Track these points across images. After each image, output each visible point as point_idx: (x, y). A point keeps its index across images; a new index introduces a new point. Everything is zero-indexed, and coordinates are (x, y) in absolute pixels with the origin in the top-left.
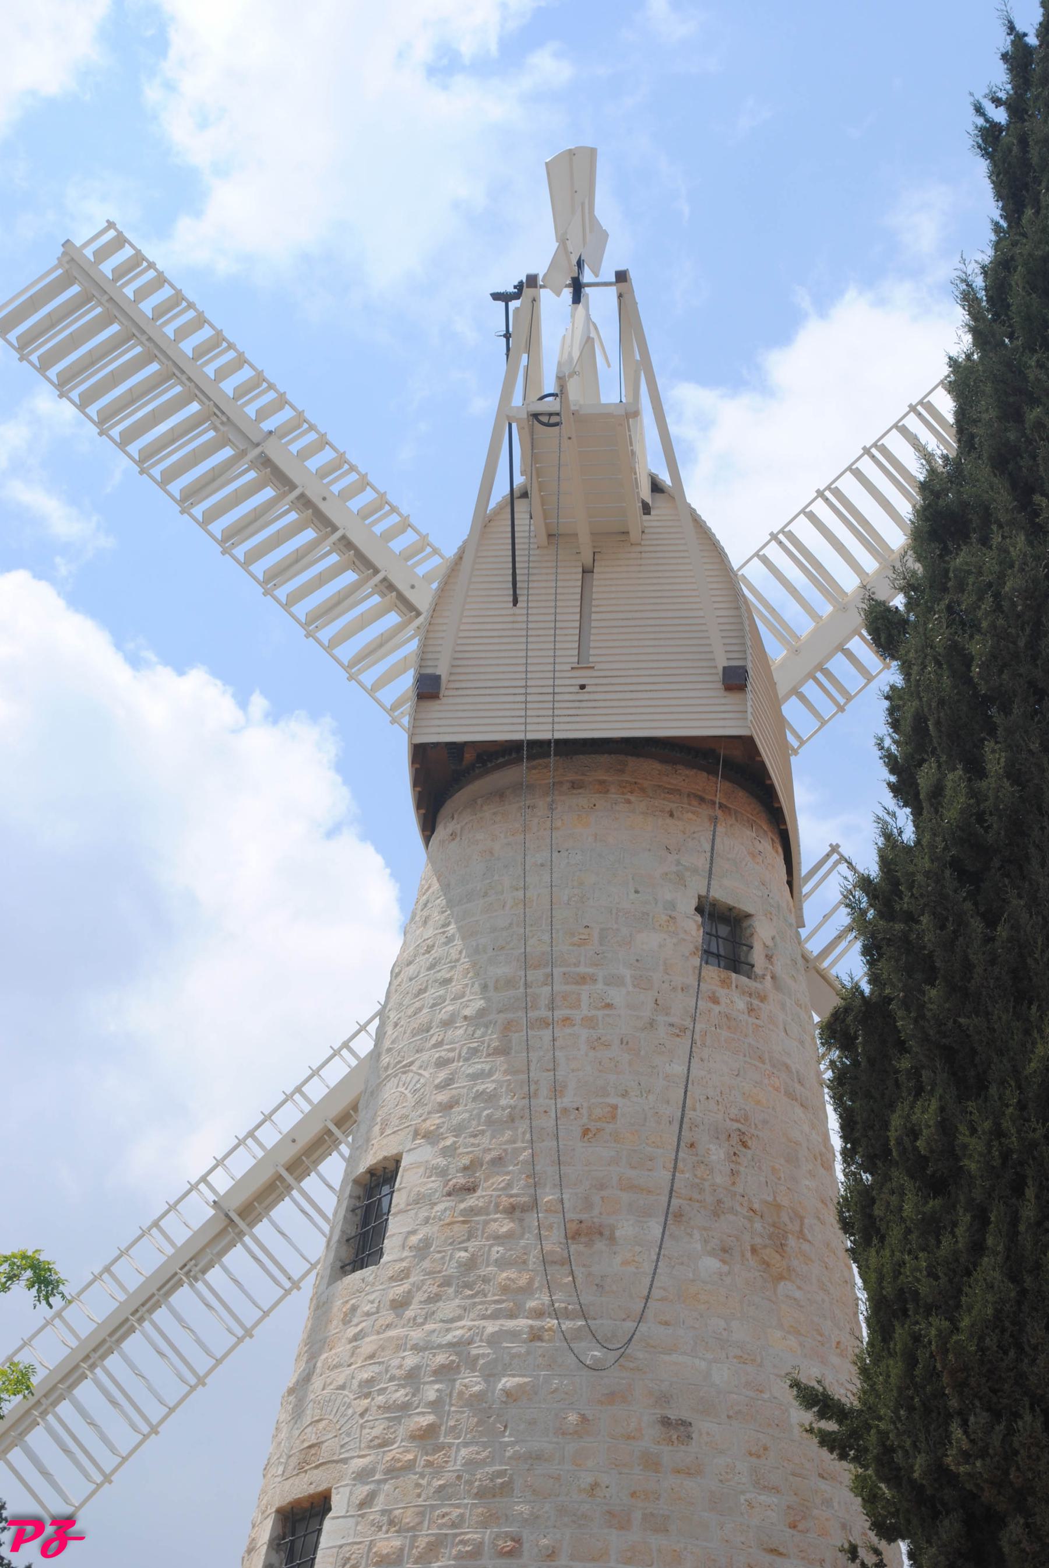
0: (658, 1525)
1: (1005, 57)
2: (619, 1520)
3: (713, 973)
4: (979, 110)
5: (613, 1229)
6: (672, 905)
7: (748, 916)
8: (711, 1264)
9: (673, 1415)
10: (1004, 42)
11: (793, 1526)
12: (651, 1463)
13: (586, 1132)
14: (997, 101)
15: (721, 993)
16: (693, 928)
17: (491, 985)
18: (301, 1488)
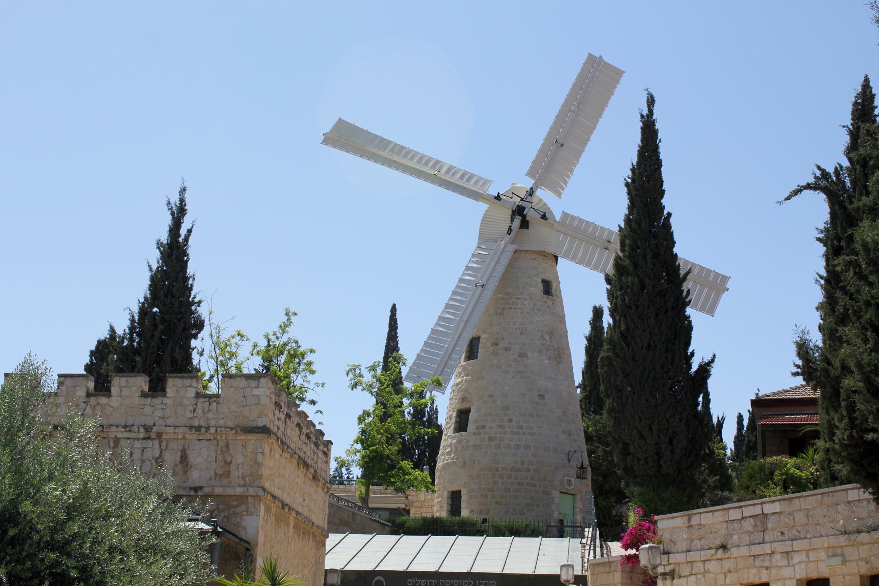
0: (538, 416)
1: (631, 169)
2: (532, 415)
3: (545, 296)
4: (625, 180)
5: (527, 354)
6: (536, 281)
7: (551, 281)
8: (547, 362)
9: (541, 394)
10: (631, 167)
11: (564, 415)
12: (537, 404)
13: (521, 333)
14: (629, 178)
15: (547, 300)
16: (541, 286)
17: (499, 299)
18: (464, 406)
